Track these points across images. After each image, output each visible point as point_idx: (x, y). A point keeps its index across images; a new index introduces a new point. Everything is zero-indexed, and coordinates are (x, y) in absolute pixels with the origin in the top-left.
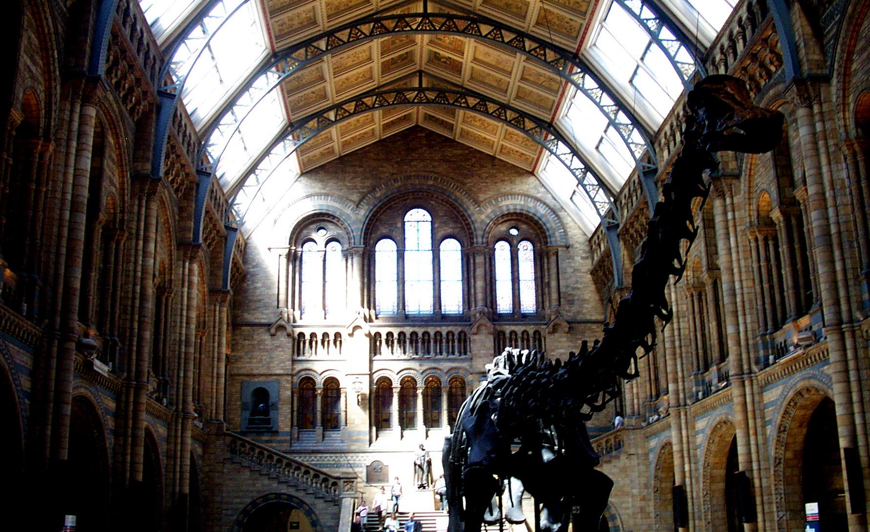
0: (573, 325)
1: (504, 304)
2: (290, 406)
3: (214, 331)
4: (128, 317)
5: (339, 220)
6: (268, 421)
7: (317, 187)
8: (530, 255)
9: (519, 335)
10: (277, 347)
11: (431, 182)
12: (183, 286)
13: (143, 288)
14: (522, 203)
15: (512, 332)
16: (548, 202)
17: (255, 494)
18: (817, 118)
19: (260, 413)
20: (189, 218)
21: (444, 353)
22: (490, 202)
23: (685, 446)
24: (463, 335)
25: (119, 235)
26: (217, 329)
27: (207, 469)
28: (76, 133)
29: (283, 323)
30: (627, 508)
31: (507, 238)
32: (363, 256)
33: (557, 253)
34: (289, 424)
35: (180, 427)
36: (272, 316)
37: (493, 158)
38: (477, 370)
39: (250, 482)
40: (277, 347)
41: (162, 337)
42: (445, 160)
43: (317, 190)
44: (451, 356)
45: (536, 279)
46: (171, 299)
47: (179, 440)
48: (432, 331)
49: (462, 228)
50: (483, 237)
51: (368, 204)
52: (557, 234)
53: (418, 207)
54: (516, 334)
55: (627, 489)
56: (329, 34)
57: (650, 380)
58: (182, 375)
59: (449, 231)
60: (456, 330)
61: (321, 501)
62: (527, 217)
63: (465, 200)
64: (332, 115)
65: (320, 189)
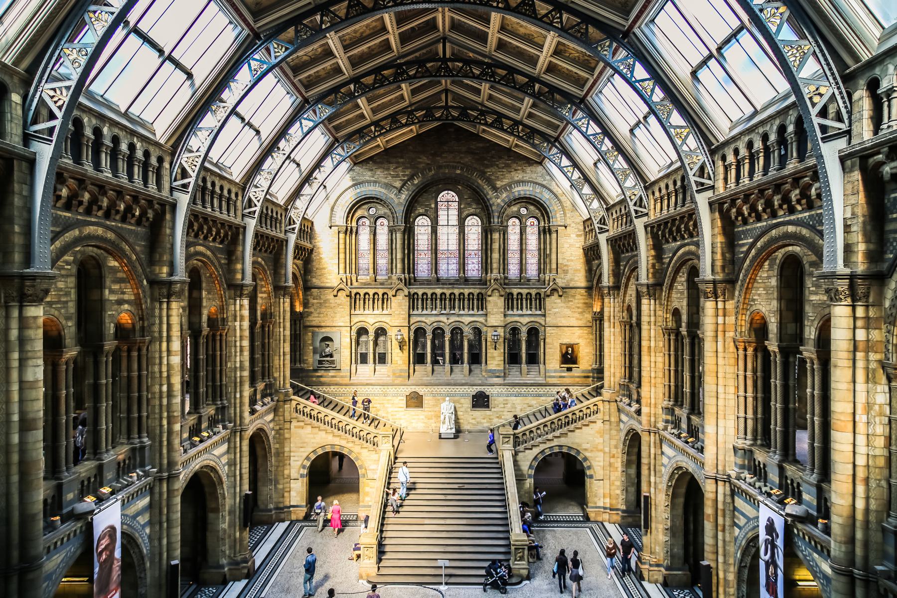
0: (567, 290)
1: (513, 271)
2: (349, 350)
3: (279, 318)
4: (157, 416)
5: (385, 203)
6: (333, 362)
7: (367, 175)
8: (536, 229)
9: (524, 296)
10: (339, 305)
11: (458, 172)
12: (235, 321)
13: (170, 386)
14: (531, 189)
15: (519, 294)
16: (552, 188)
17: (315, 445)
18: (859, 323)
19: (327, 356)
20: (237, 260)
21: (466, 310)
22: (506, 189)
23: (652, 462)
24: (480, 296)
25: (140, 343)
26: (282, 318)
27: (278, 428)
28: (17, 342)
29: (342, 286)
30: (599, 461)
31: (518, 216)
32: (404, 233)
33: (557, 231)
34: (349, 363)
35: (238, 439)
36: (335, 280)
37: (509, 150)
38: (490, 325)
39: (312, 436)
40: (339, 305)
41: (219, 368)
42: (470, 152)
43: (368, 178)
44: (471, 312)
45: (539, 249)
46: (224, 334)
47: (238, 450)
48: (457, 292)
49: (482, 209)
50: (498, 218)
51: (408, 190)
52: (558, 215)
53: (448, 190)
54: (521, 294)
55: (601, 447)
56: (355, 80)
57: (625, 363)
58: (238, 395)
59: (472, 211)
60: (476, 291)
61: (366, 450)
62: (535, 200)
63: (485, 187)
64: (373, 128)
65: (370, 177)
